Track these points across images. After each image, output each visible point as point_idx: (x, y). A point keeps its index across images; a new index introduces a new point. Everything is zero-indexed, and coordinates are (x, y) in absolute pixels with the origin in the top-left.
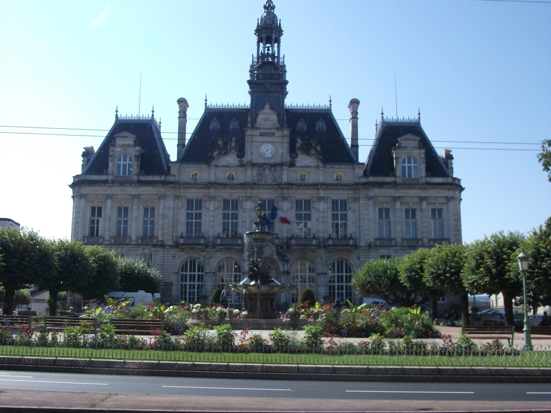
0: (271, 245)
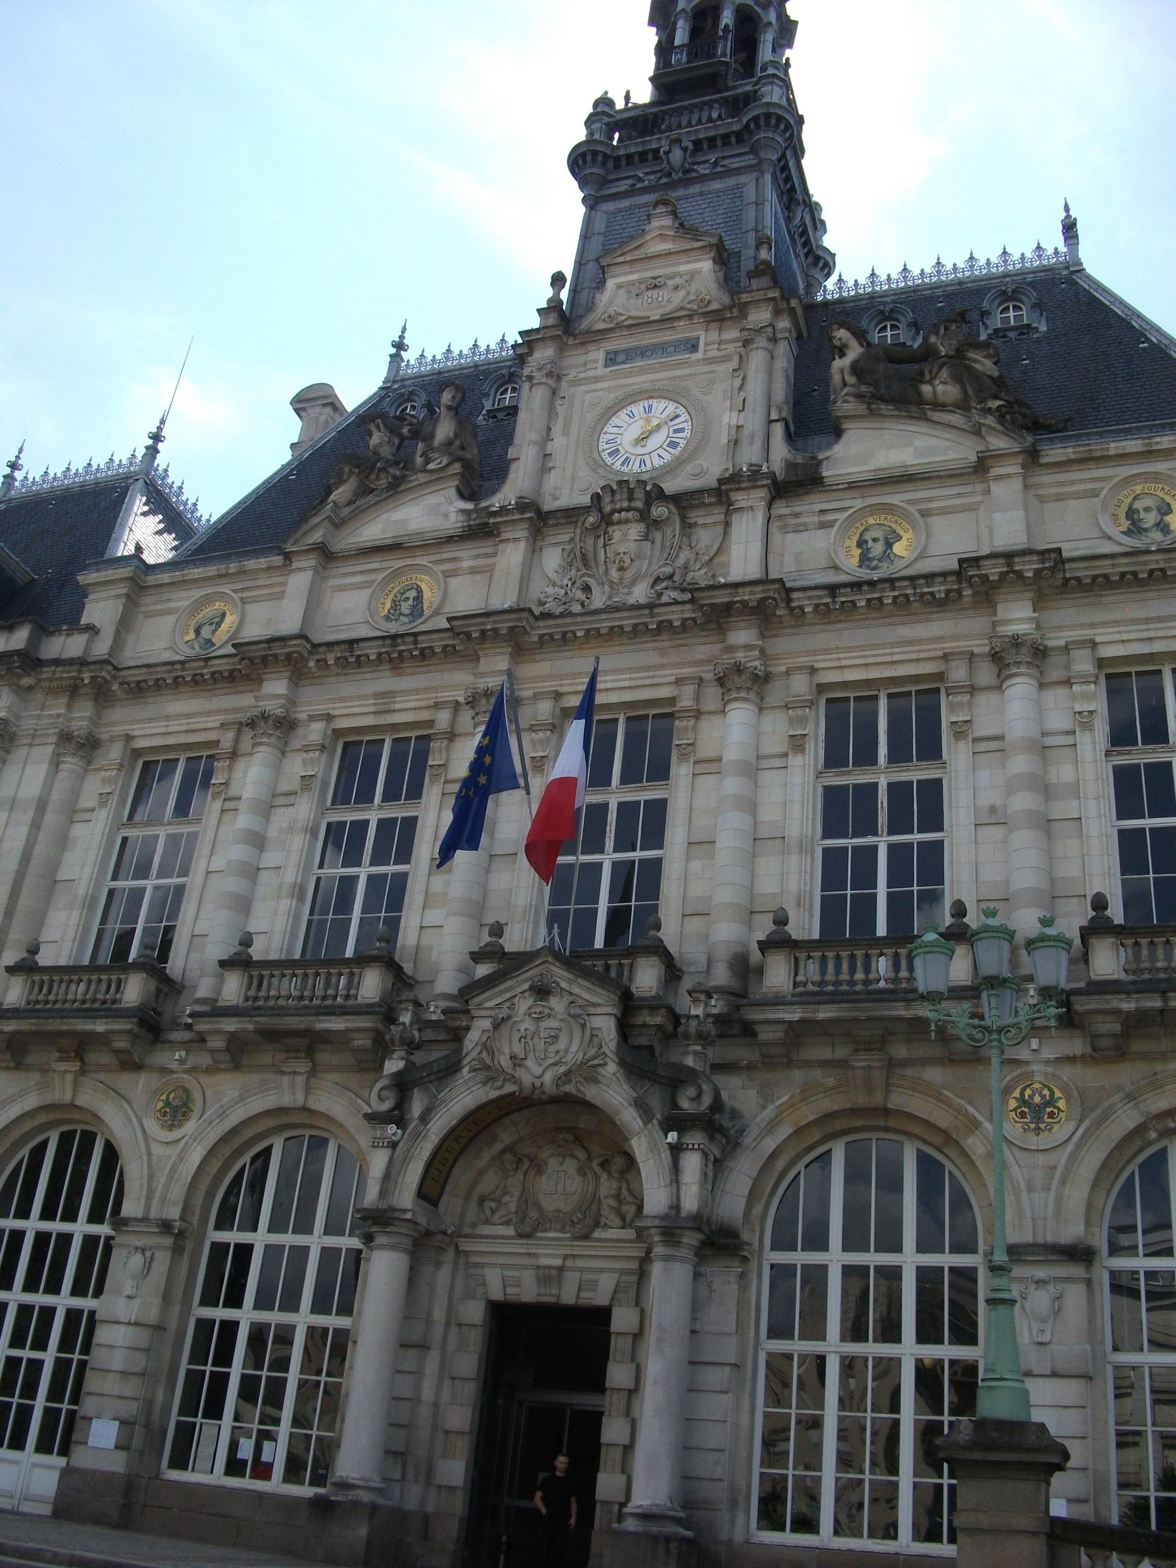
0: (584, 990)
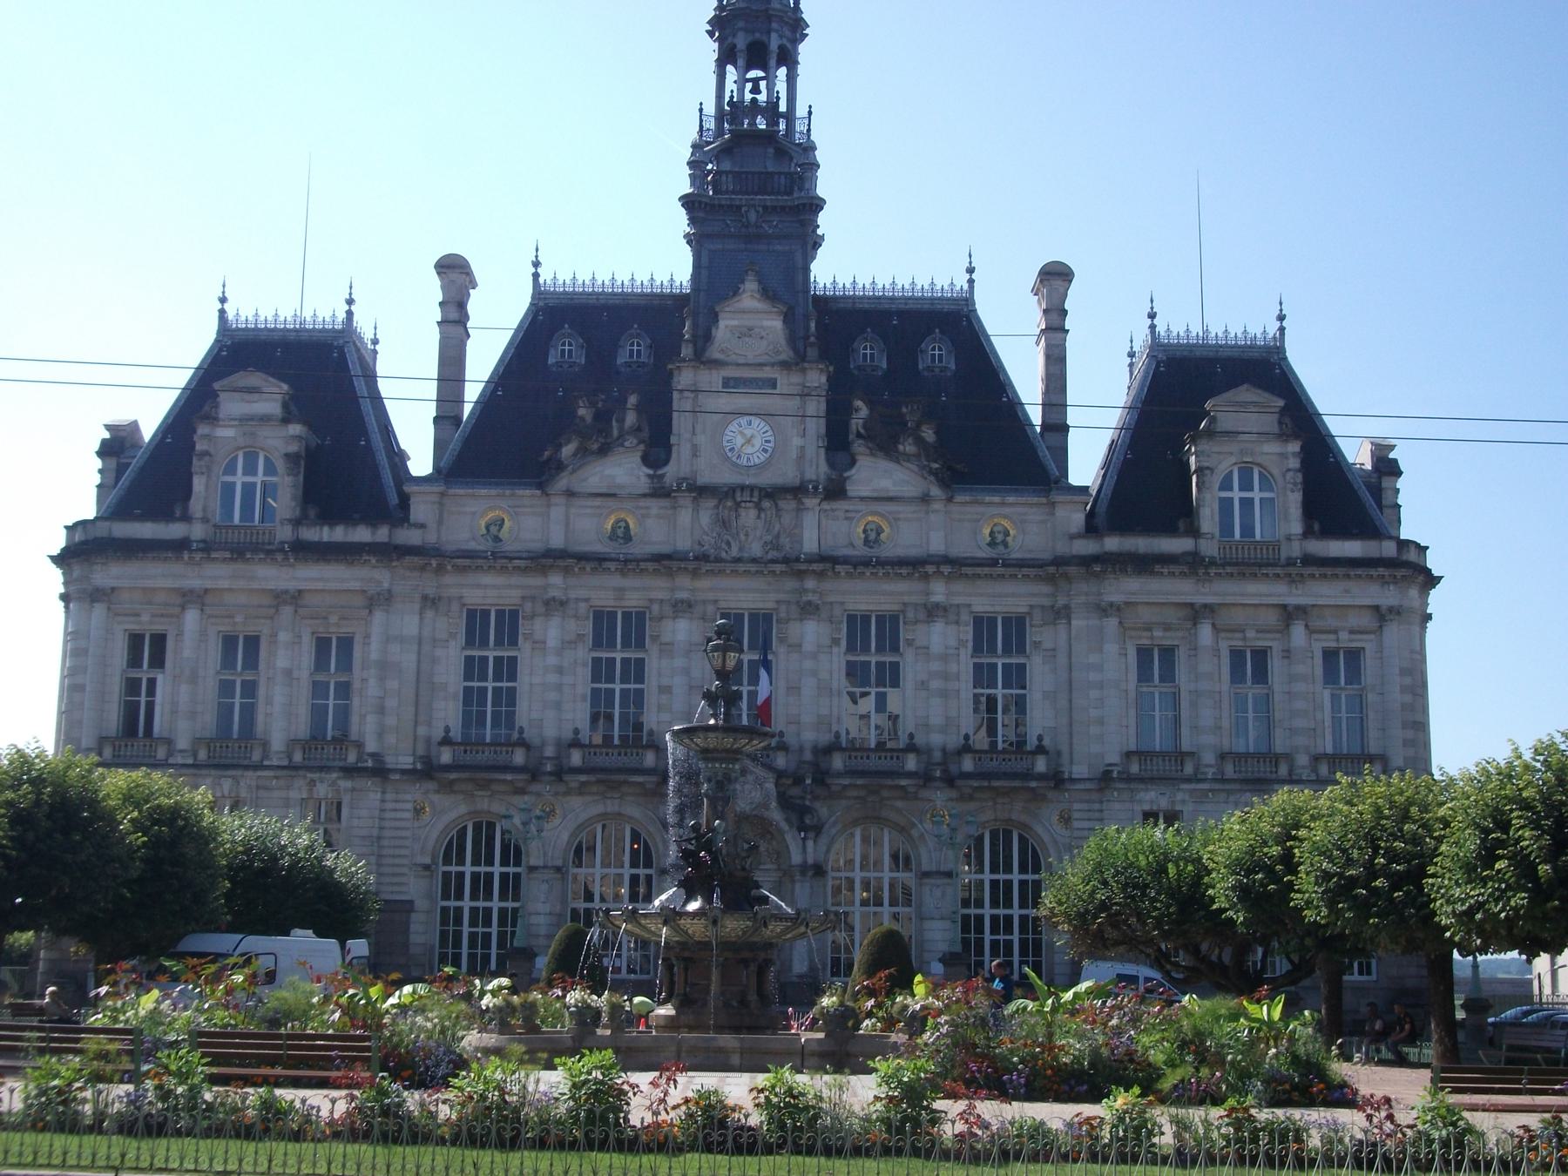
0: (759, 771)
